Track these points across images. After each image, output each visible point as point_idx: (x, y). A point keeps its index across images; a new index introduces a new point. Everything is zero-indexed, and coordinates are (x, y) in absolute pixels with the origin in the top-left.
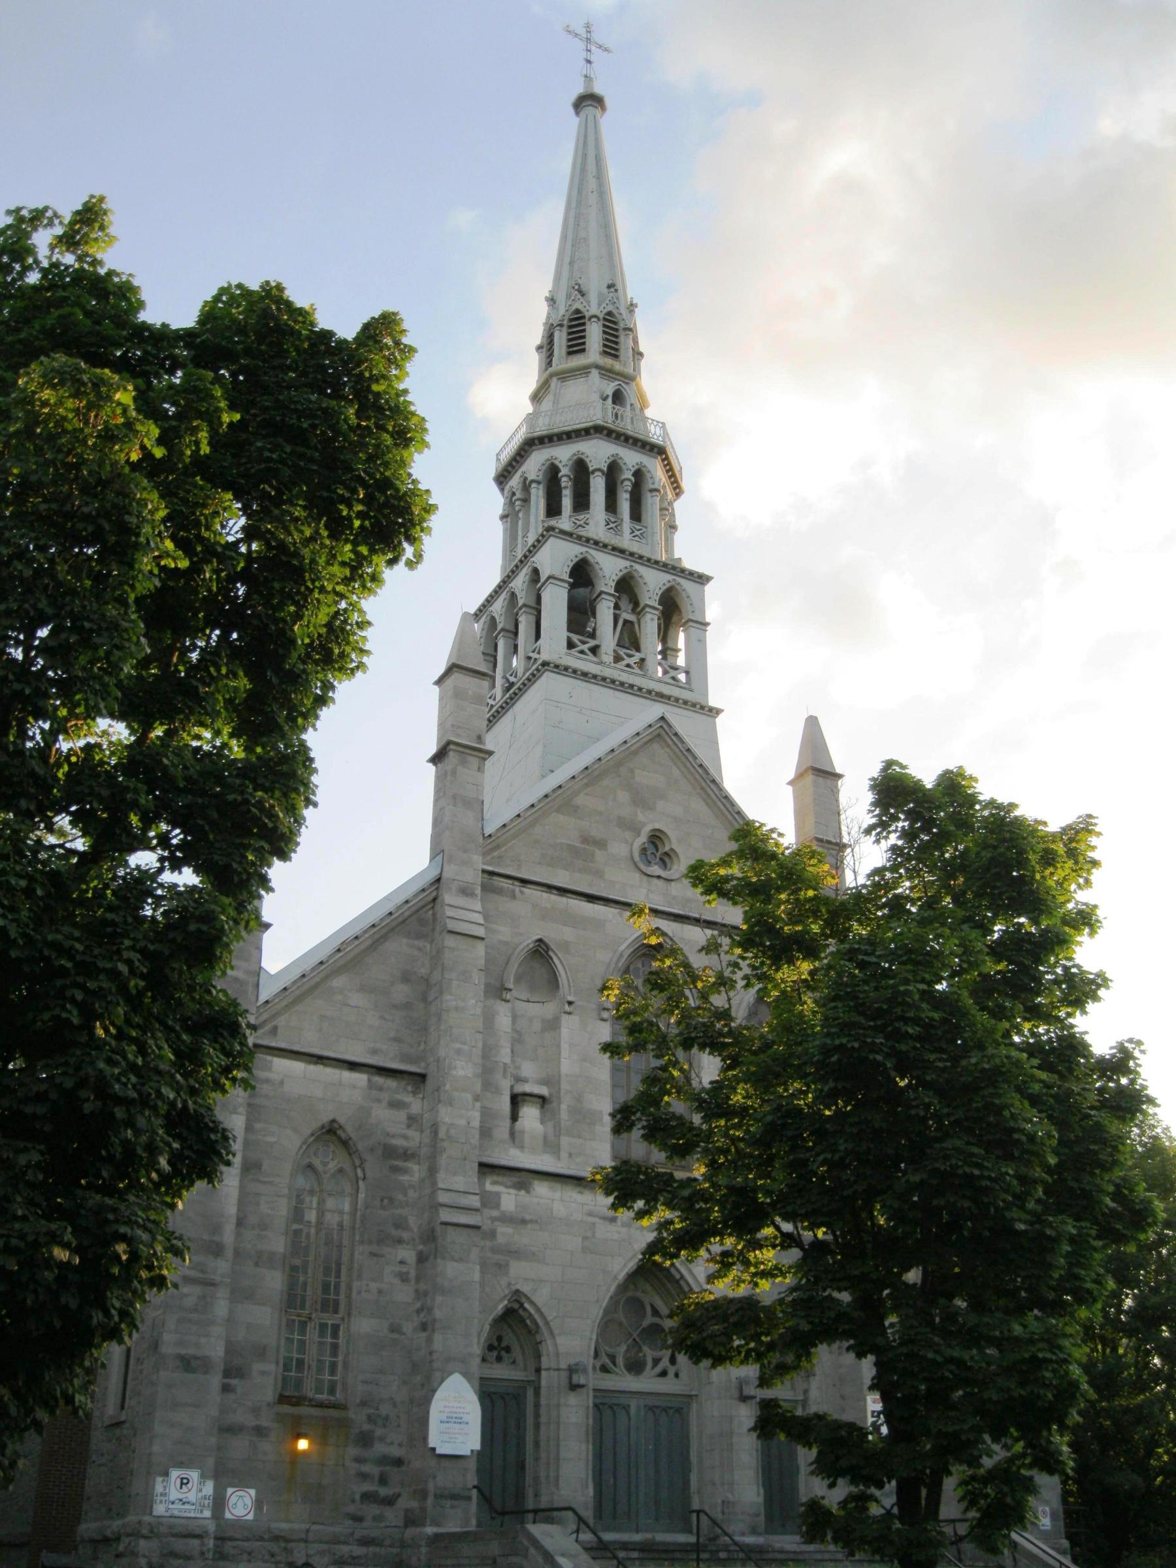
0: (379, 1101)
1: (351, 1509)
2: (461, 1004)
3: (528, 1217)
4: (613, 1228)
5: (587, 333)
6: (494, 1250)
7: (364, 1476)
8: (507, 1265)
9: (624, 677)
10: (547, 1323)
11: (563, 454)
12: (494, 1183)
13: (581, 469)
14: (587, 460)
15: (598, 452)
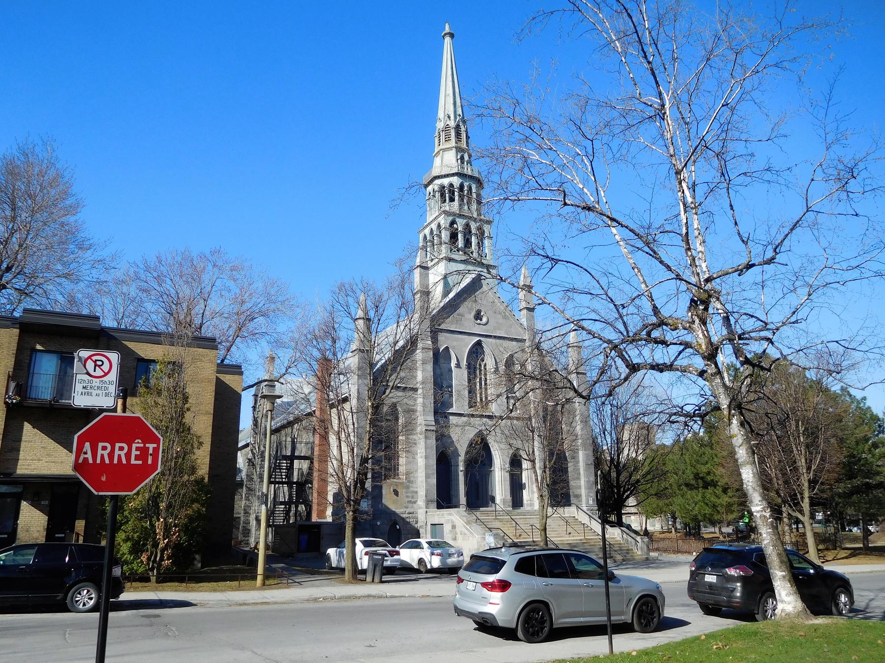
7: (408, 497)
11: (446, 182)
13: (451, 185)
15: (456, 181)
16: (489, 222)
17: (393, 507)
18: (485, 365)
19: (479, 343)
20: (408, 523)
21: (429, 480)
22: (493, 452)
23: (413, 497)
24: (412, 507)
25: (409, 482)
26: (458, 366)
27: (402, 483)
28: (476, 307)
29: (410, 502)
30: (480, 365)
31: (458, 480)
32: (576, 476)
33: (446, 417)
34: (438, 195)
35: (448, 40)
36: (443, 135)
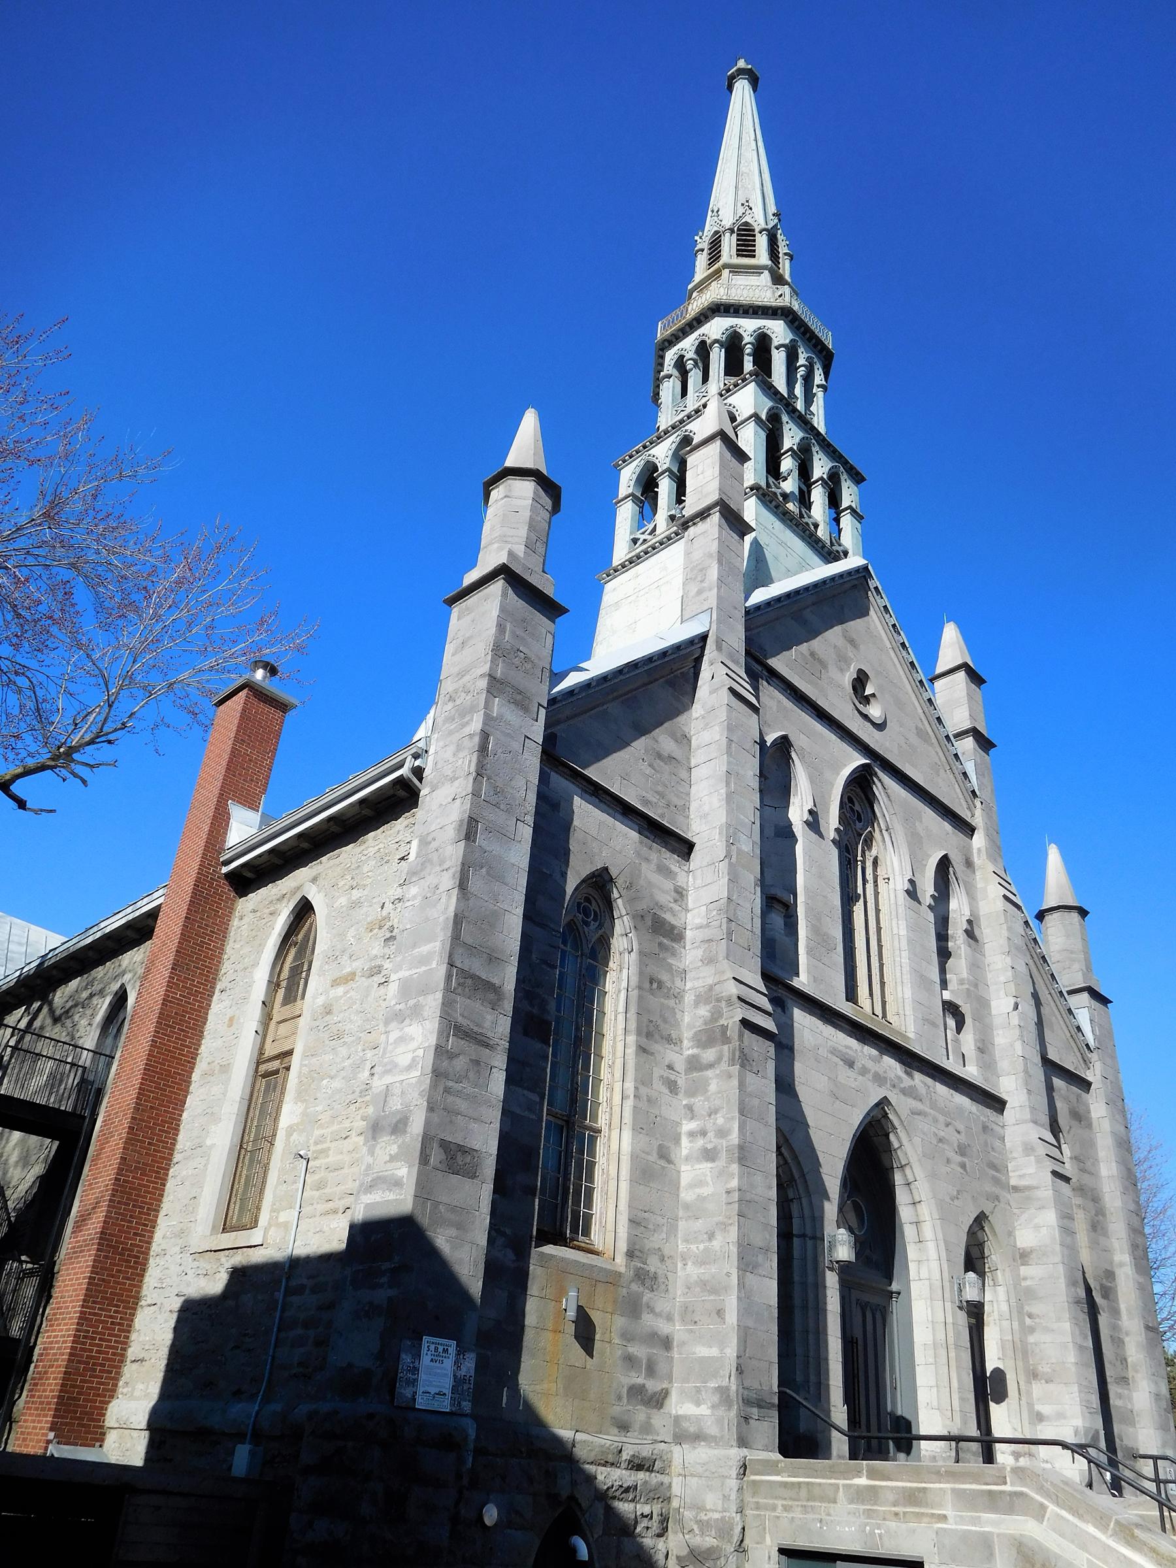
0: (647, 860)
1: (616, 1410)
2: (741, 772)
5: (756, 243)
10: (803, 1175)
11: (748, 327)
14: (773, 336)
15: (779, 331)
16: (858, 478)
17: (560, 1420)
18: (875, 862)
20: (624, 1530)
22: (905, 1213)
23: (651, 1371)
24: (647, 1428)
25: (641, 1276)
26: (814, 823)
27: (612, 1279)
29: (636, 1392)
34: (717, 357)
35: (742, 88)
36: (729, 244)
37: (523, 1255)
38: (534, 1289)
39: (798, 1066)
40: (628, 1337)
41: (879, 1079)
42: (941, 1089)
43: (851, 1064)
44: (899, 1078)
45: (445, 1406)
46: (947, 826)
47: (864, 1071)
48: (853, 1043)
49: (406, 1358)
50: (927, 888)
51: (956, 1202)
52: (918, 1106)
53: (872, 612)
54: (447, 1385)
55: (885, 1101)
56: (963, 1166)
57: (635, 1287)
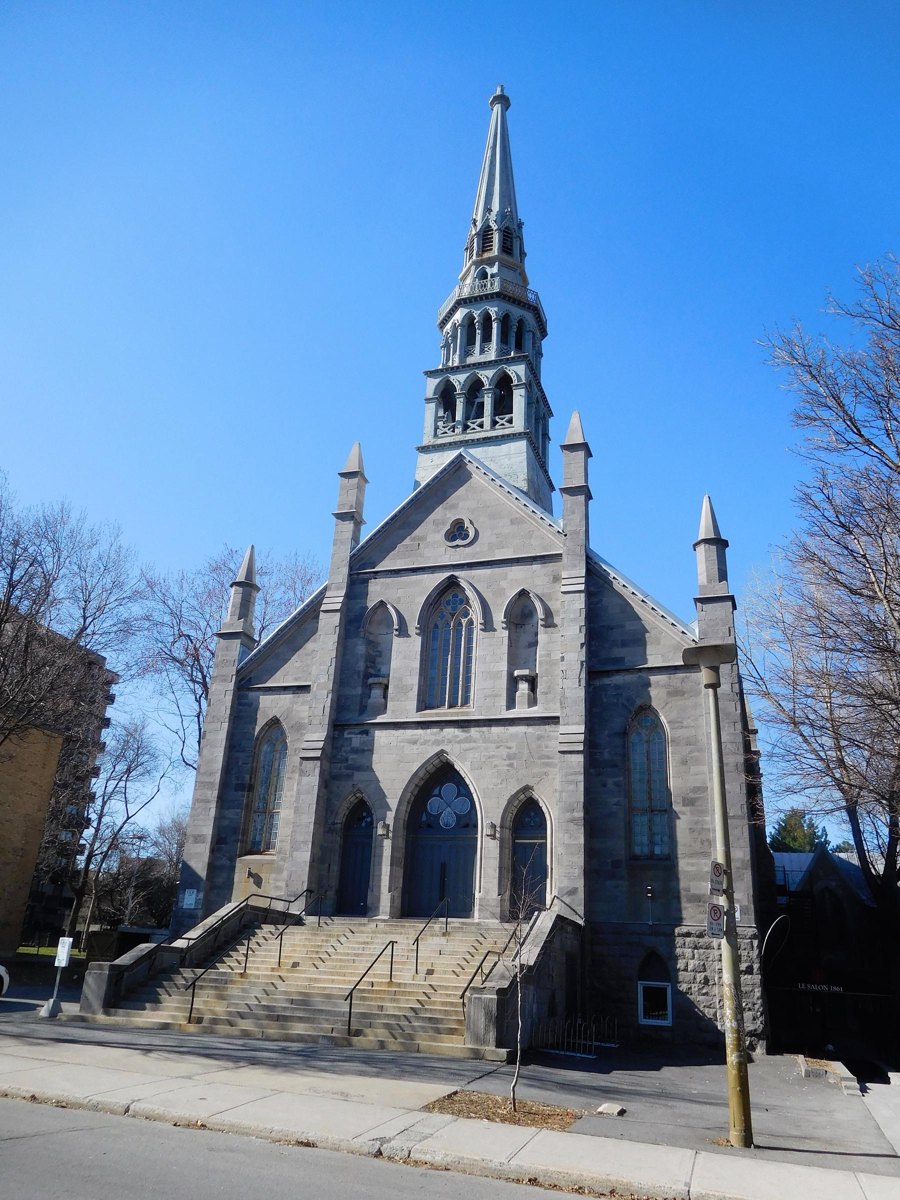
3: (366, 748)
4: (415, 747)
6: (347, 768)
8: (353, 775)
9: (507, 432)
12: (350, 733)
19: (452, 584)
21: (295, 854)
28: (452, 517)
30: (460, 624)
31: (381, 856)
32: (697, 847)
33: (366, 733)
37: (233, 860)
38: (237, 870)
39: (375, 757)
40: (276, 880)
41: (437, 743)
42: (496, 730)
43: (415, 742)
44: (457, 736)
45: (193, 907)
46: (536, 567)
47: (426, 742)
48: (420, 732)
49: (181, 896)
50: (499, 617)
51: (499, 786)
52: (472, 745)
53: (474, 475)
54: (193, 902)
55: (442, 751)
56: (511, 765)
57: (281, 863)
